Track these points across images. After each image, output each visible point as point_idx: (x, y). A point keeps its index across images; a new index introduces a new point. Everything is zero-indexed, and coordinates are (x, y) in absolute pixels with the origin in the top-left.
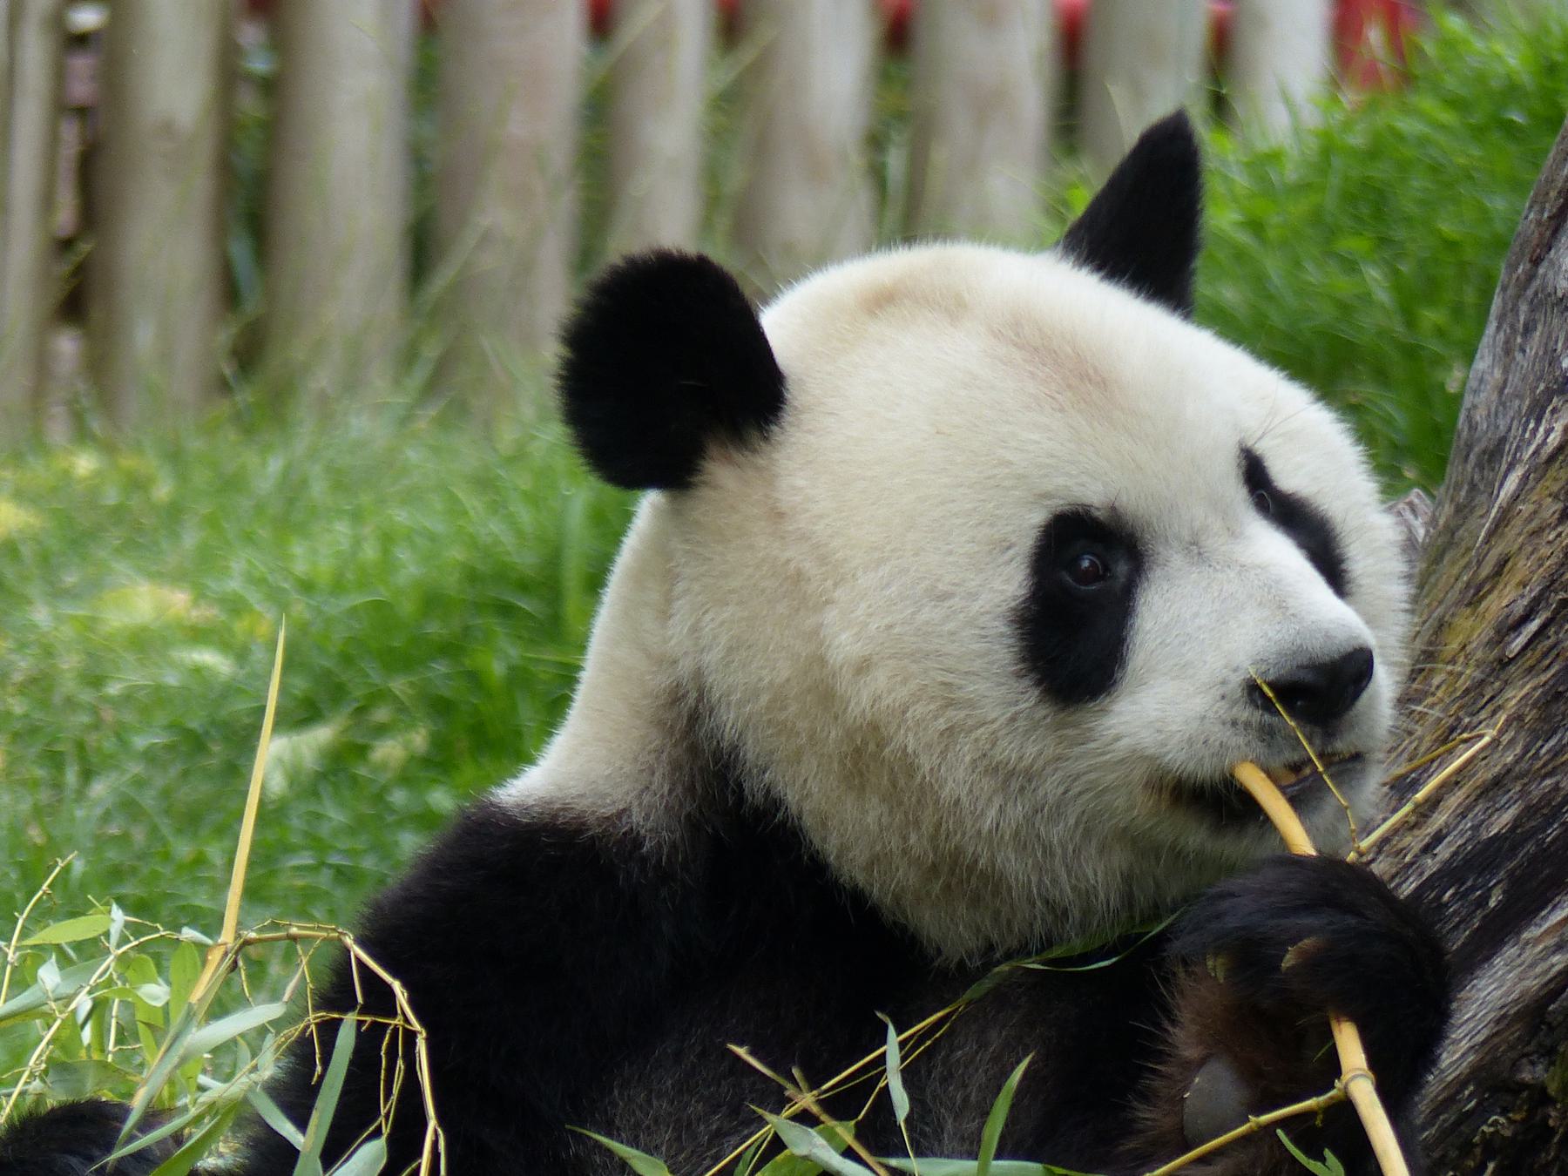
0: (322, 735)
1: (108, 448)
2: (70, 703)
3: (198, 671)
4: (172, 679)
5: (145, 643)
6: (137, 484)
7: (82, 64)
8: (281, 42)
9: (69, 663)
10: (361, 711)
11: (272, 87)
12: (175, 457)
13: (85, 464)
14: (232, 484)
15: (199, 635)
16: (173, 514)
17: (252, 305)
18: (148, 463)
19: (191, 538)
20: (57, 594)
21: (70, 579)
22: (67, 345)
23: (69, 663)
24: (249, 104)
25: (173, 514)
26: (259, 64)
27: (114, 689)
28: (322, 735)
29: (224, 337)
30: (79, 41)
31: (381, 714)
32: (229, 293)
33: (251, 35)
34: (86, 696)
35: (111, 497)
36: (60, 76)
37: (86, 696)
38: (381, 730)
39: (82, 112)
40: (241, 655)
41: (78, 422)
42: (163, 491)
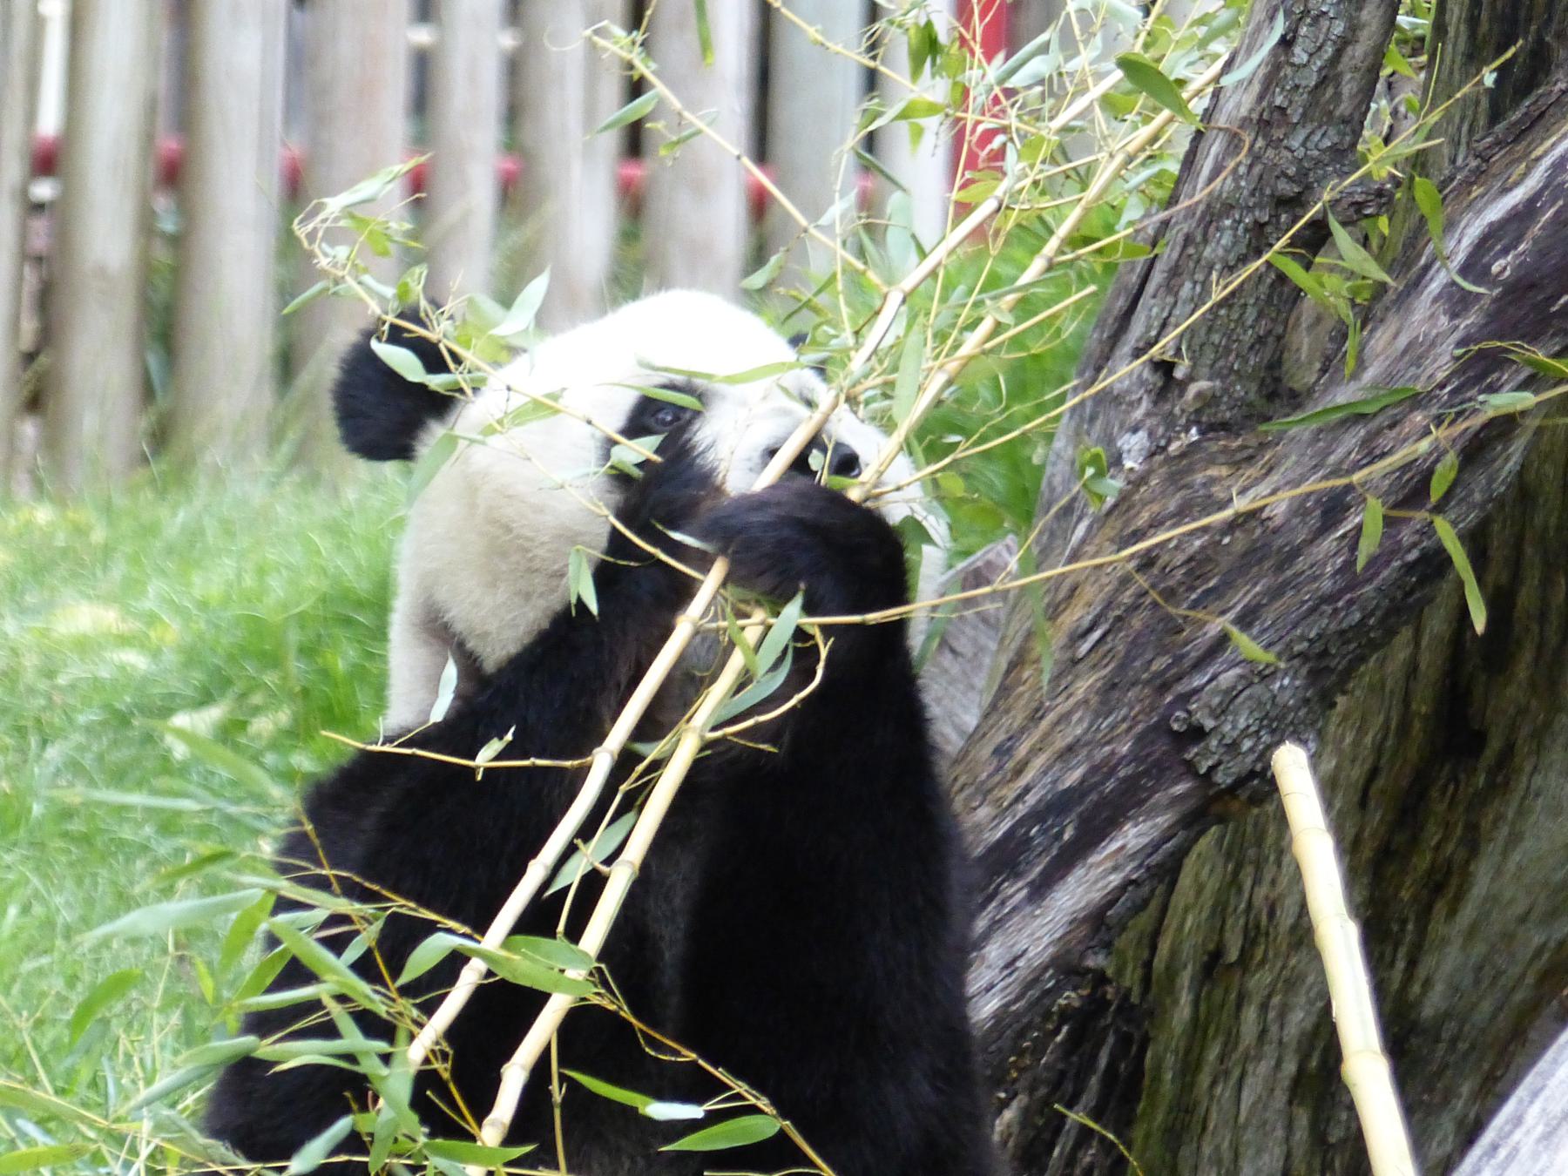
0: (213, 715)
1: (60, 502)
2: (31, 691)
3: (122, 668)
4: (104, 673)
5: (85, 646)
6: (80, 531)
7: (40, 225)
8: (187, 211)
9: (30, 661)
10: (243, 696)
11: (178, 242)
12: (107, 509)
13: (43, 515)
14: (150, 530)
15: (124, 641)
16: (107, 551)
17: (162, 402)
18: (86, 515)
19: (119, 570)
20: (23, 610)
21: (30, 599)
22: (29, 429)
23: (30, 661)
24: (162, 254)
25: (107, 551)
26: (168, 225)
27: (62, 680)
28: (213, 715)
29: (144, 423)
30: (38, 208)
31: (257, 699)
32: (147, 392)
33: (163, 203)
34: (43, 685)
35: (60, 540)
36: (23, 235)
37: (43, 685)
38: (256, 711)
39: (39, 260)
40: (156, 654)
41: (38, 485)
42: (98, 535)
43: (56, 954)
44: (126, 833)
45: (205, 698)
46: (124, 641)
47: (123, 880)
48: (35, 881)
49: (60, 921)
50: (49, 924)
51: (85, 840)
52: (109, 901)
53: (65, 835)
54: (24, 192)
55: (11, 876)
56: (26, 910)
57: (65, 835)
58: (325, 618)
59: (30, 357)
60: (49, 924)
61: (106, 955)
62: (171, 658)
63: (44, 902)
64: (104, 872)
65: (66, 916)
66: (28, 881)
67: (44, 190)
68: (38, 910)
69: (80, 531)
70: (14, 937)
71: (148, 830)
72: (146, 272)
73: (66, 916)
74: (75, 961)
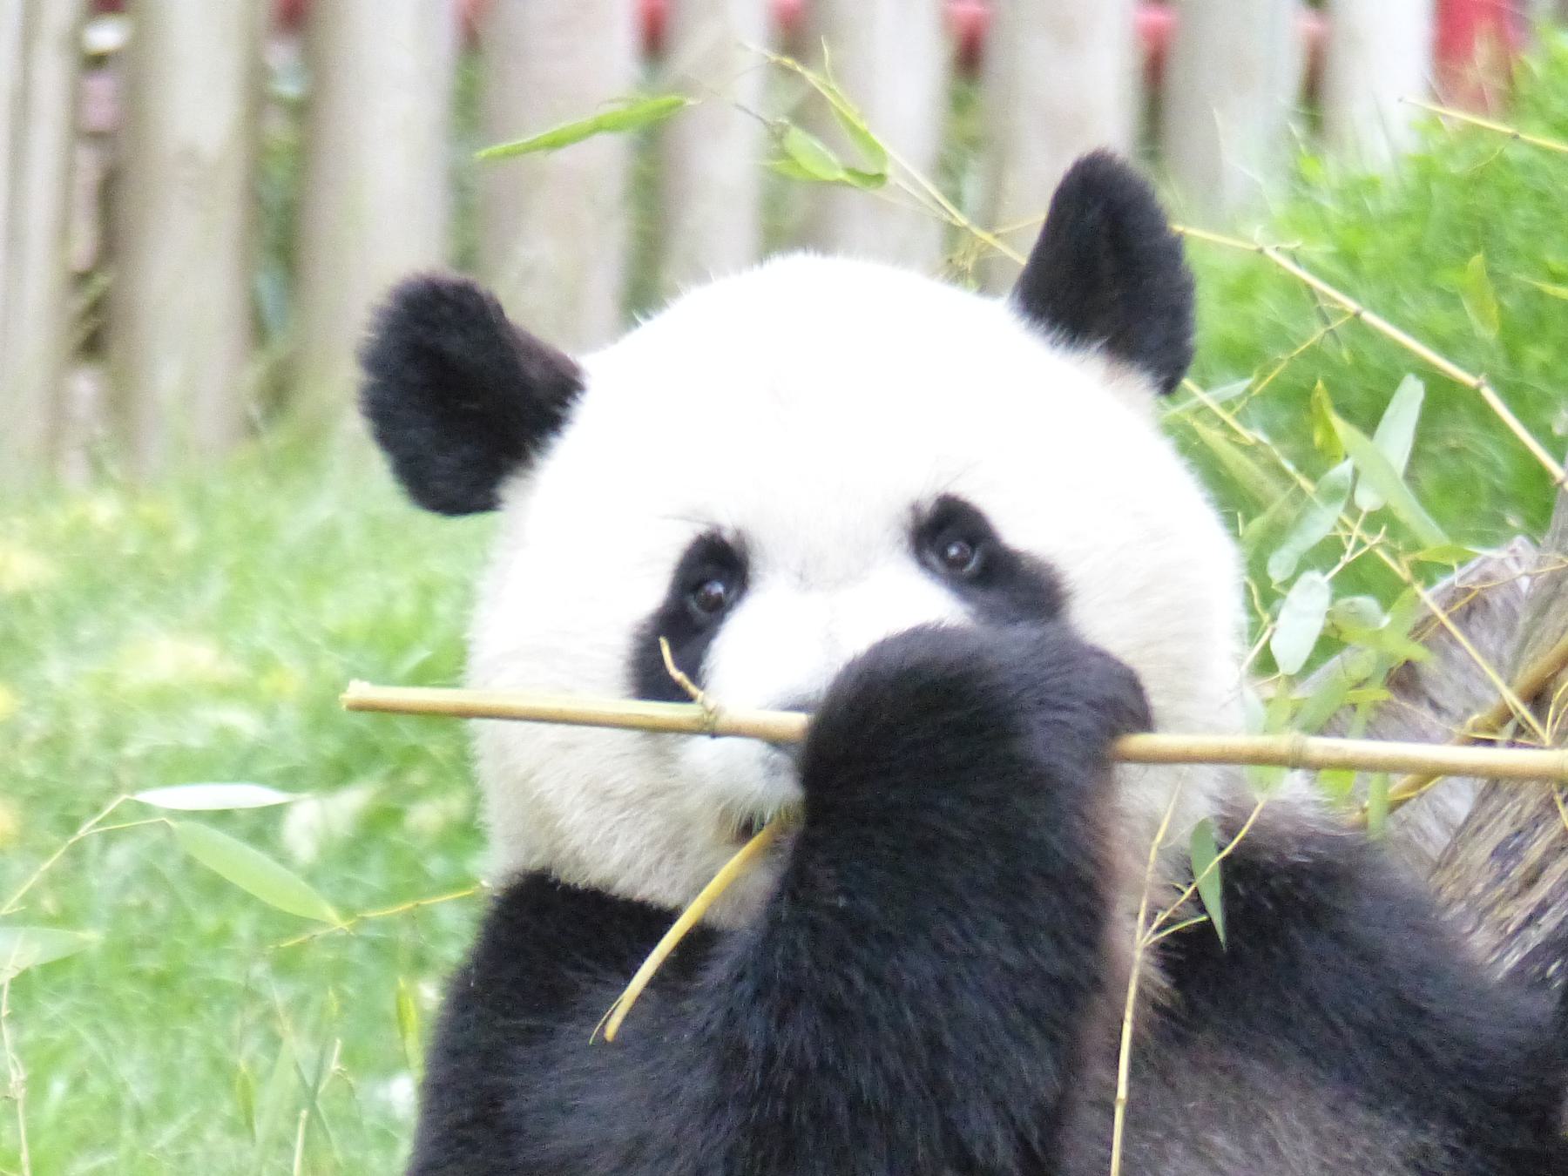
0: (354, 799)
1: (130, 492)
2: (87, 765)
3: (224, 733)
4: (195, 741)
5: (166, 701)
6: (159, 534)
7: (101, 87)
8: (315, 65)
9: (86, 723)
10: (396, 774)
11: (303, 111)
12: (199, 502)
13: (104, 510)
14: (258, 533)
15: (226, 692)
16: (199, 563)
17: (280, 346)
18: (168, 508)
19: (216, 589)
20: (74, 648)
21: (85, 633)
22: (85, 385)
23: (86, 723)
24: (278, 129)
25: (199, 563)
26: (289, 88)
27: (132, 750)
28: (354, 799)
29: (253, 374)
30: (97, 62)
31: (417, 777)
32: (258, 330)
33: (281, 55)
34: (103, 758)
35: (130, 549)
36: (77, 101)
37: (103, 758)
38: (415, 795)
39: (97, 137)
40: (270, 714)
41: (96, 466)
42: (186, 540)
43: (123, 1150)
44: (227, 973)
45: (339, 774)
46: (226, 692)
47: (219, 1042)
48: (93, 1043)
49: (127, 1102)
50: (113, 1105)
51: (161, 983)
52: (201, 1070)
53: (136, 975)
54: (74, 40)
55: (59, 1037)
56: (77, 1084)
57: (136, 975)
58: (966, 682)
59: (82, 279)
60: (113, 1105)
61: (195, 1149)
62: (290, 717)
63: (105, 1073)
64: (192, 1030)
65: (139, 1093)
66: (79, 1043)
67: (106, 36)
68: (96, 1085)
69: (159, 534)
70: (60, 1125)
71: (259, 969)
72: (258, 156)
73: (139, 1093)
74: (151, 1160)
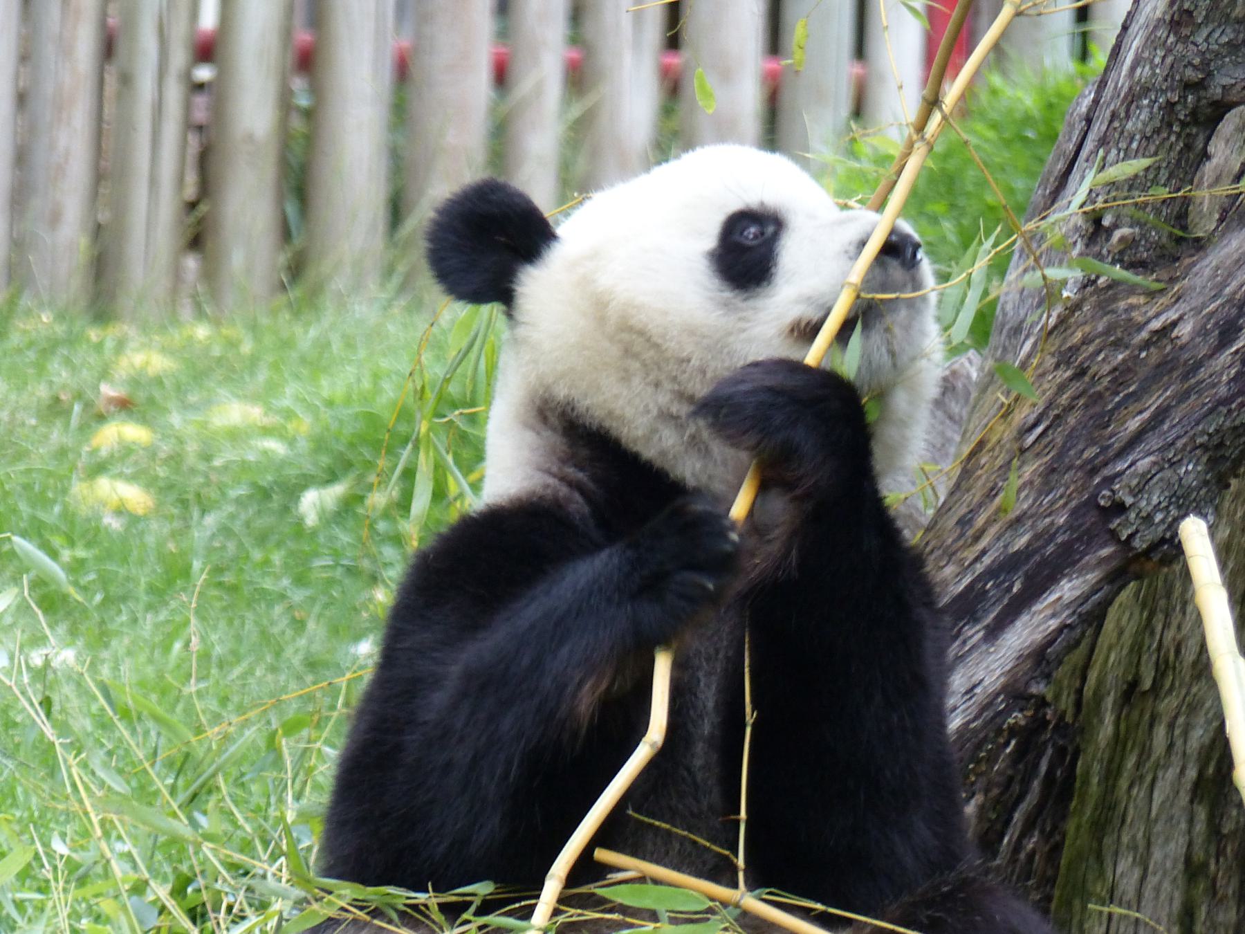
0: (337, 490)
1: (216, 322)
2: (193, 471)
3: (265, 452)
4: (251, 457)
5: (236, 436)
6: (233, 344)
7: (200, 100)
8: (316, 90)
9: (192, 448)
11: (309, 115)
12: (254, 328)
13: (202, 332)
14: (287, 344)
15: (267, 431)
16: (253, 362)
17: (298, 241)
18: (236, 331)
19: (262, 376)
20: (185, 407)
21: (193, 398)
22: (191, 263)
23: (192, 448)
24: (297, 124)
26: (303, 101)
27: (217, 462)
28: (337, 490)
29: (282, 259)
30: (200, 87)
31: (372, 478)
32: (286, 234)
33: (298, 84)
34: (202, 466)
35: (217, 351)
36: (188, 108)
37: (202, 466)
38: (370, 487)
39: (200, 128)
40: (292, 442)
42: (247, 348)
43: (212, 681)
44: (268, 584)
45: (331, 477)
47: (265, 622)
51: (233, 589)
52: (255, 637)
54: (187, 76)
59: (192, 206)
61: (251, 680)
62: (303, 445)
64: (249, 615)
65: (218, 650)
67: (204, 73)
71: (285, 582)
72: (285, 137)
74: (227, 686)
